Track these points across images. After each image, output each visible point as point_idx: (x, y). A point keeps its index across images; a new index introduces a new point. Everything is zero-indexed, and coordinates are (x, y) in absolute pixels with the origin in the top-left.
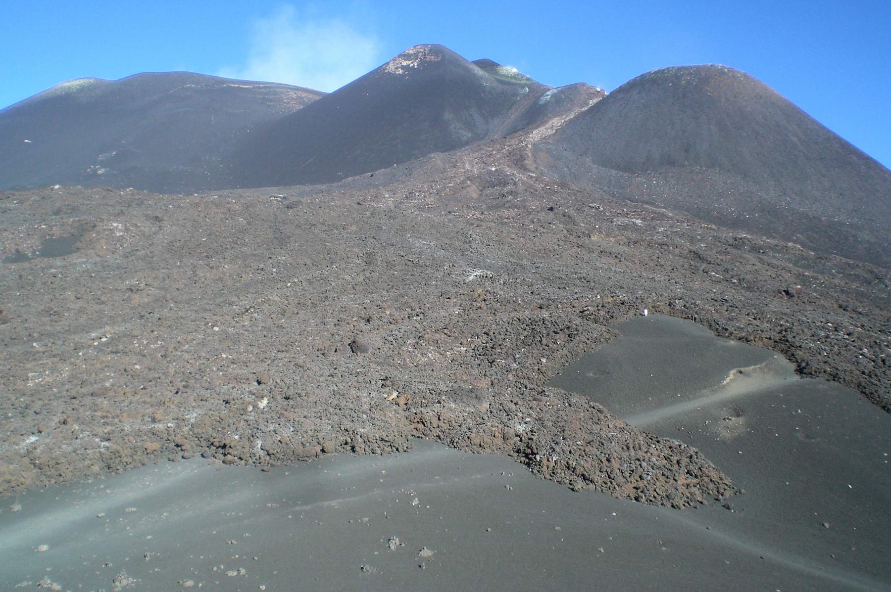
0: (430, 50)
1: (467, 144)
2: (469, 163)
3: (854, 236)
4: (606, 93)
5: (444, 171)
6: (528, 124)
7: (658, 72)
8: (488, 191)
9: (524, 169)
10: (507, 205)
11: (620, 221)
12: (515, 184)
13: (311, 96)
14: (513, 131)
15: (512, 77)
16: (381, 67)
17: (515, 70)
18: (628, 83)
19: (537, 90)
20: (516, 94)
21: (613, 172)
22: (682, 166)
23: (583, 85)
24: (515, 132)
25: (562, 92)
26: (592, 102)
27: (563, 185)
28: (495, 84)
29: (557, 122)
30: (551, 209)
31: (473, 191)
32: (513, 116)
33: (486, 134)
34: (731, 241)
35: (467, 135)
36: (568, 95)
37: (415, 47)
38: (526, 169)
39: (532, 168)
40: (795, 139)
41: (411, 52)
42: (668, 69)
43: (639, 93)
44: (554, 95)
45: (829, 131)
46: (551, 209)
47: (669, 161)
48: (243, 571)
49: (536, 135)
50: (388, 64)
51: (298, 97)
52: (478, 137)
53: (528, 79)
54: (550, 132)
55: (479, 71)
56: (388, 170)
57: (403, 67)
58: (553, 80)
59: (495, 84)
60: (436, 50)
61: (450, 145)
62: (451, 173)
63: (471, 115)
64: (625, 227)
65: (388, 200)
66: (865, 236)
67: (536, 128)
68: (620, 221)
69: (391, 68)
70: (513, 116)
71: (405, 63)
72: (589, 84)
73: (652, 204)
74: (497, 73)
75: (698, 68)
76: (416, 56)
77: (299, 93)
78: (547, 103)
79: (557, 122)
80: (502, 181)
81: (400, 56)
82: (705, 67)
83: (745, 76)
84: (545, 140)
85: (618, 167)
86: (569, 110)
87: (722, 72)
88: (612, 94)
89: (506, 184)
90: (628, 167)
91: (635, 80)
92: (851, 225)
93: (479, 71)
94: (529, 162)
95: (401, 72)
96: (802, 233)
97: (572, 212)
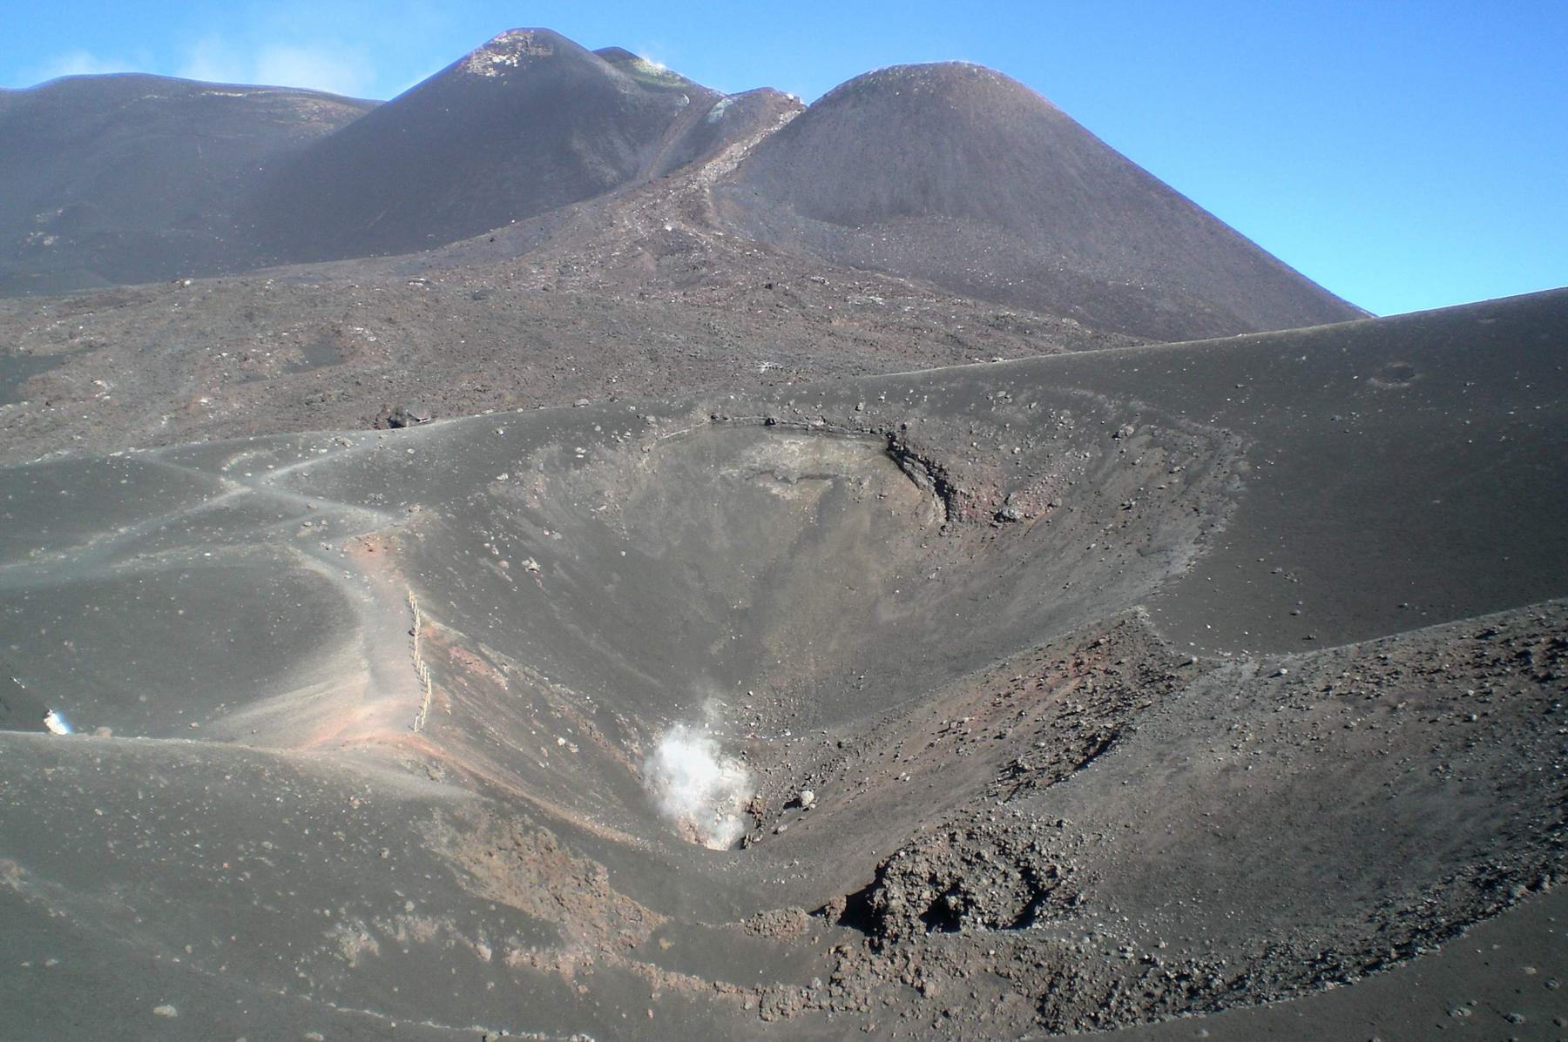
0: (535, 38)
1: (613, 186)
2: (629, 222)
3: (1149, 306)
4: (807, 101)
5: (598, 233)
6: (697, 154)
7: (878, 73)
8: (668, 260)
9: (708, 226)
10: (703, 280)
11: (854, 299)
12: (702, 249)
13: (340, 107)
14: (674, 167)
15: (662, 77)
16: (455, 65)
17: (660, 67)
18: (836, 90)
19: (703, 99)
20: (672, 108)
21: (827, 226)
22: (920, 214)
23: (769, 90)
24: (680, 166)
25: (738, 103)
26: (787, 117)
27: (764, 247)
28: (639, 92)
29: (737, 150)
30: (770, 286)
31: (647, 260)
32: (672, 142)
33: (636, 170)
34: (992, 321)
35: (611, 174)
36: (751, 105)
37: (509, 32)
38: (708, 226)
39: (716, 224)
40: (1073, 171)
41: (504, 40)
42: (893, 68)
43: (854, 106)
44: (728, 109)
45: (1120, 156)
46: (770, 286)
47: (901, 208)
48: (248, 875)
49: (711, 171)
50: (468, 58)
51: (322, 110)
52: (626, 177)
53: (683, 80)
54: (730, 167)
55: (610, 70)
56: (507, 229)
57: (495, 66)
58: (722, 77)
59: (639, 92)
60: (543, 38)
61: (592, 189)
62: (608, 234)
63: (611, 142)
64: (862, 308)
65: (539, 278)
66: (1165, 304)
67: (709, 159)
68: (854, 299)
69: (476, 66)
70: (672, 142)
71: (497, 59)
72: (777, 89)
73: (884, 271)
74: (634, 72)
75: (935, 66)
76: (510, 48)
77: (323, 104)
78: (720, 121)
79: (737, 150)
80: (682, 245)
81: (488, 46)
82: (946, 64)
83: (1002, 78)
84: (724, 178)
85: (830, 218)
86: (752, 132)
87: (969, 73)
88: (816, 107)
89: (689, 250)
90: (845, 218)
91: (845, 86)
92: (1148, 291)
93: (610, 70)
94: (710, 215)
95: (491, 73)
96: (1081, 304)
97: (794, 290)
